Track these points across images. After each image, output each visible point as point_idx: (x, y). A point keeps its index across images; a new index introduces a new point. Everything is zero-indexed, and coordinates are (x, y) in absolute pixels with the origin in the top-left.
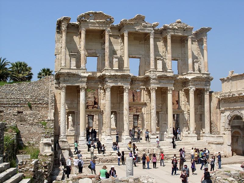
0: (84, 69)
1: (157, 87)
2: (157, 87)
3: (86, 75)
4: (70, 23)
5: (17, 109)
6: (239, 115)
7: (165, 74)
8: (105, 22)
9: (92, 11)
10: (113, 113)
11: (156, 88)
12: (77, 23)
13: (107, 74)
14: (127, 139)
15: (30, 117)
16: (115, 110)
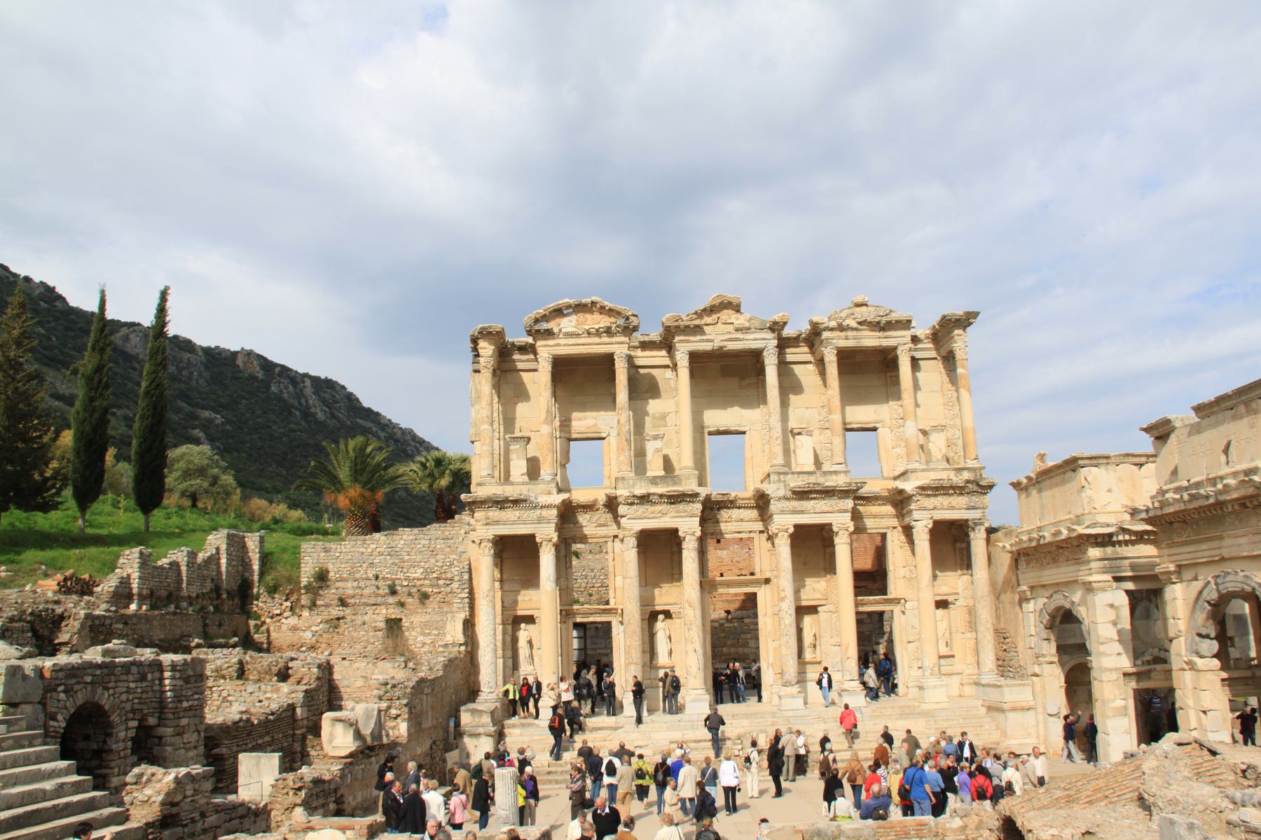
0: (549, 482)
1: (796, 526)
2: (796, 526)
3: (558, 499)
4: (513, 344)
5: (384, 611)
6: (1067, 606)
7: (821, 480)
8: (609, 328)
9: (567, 300)
10: (661, 617)
11: (791, 530)
12: (530, 340)
13: (622, 493)
14: (694, 701)
15: (424, 634)
16: (666, 608)
